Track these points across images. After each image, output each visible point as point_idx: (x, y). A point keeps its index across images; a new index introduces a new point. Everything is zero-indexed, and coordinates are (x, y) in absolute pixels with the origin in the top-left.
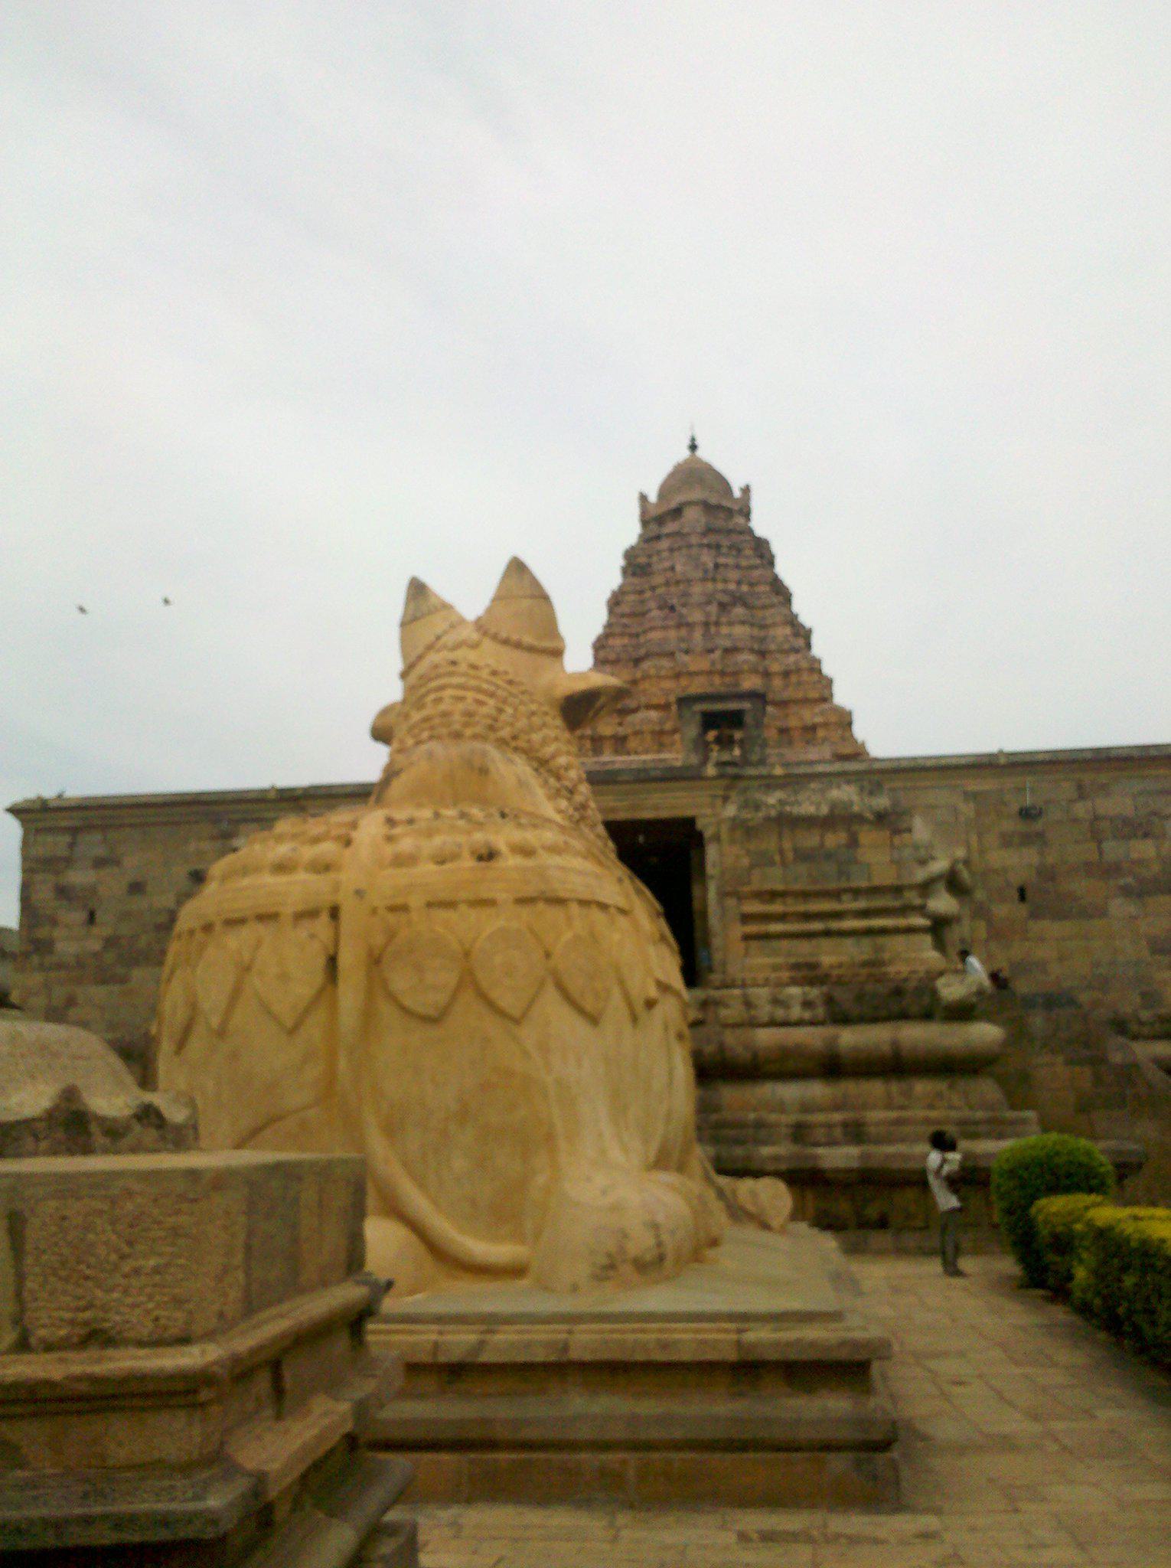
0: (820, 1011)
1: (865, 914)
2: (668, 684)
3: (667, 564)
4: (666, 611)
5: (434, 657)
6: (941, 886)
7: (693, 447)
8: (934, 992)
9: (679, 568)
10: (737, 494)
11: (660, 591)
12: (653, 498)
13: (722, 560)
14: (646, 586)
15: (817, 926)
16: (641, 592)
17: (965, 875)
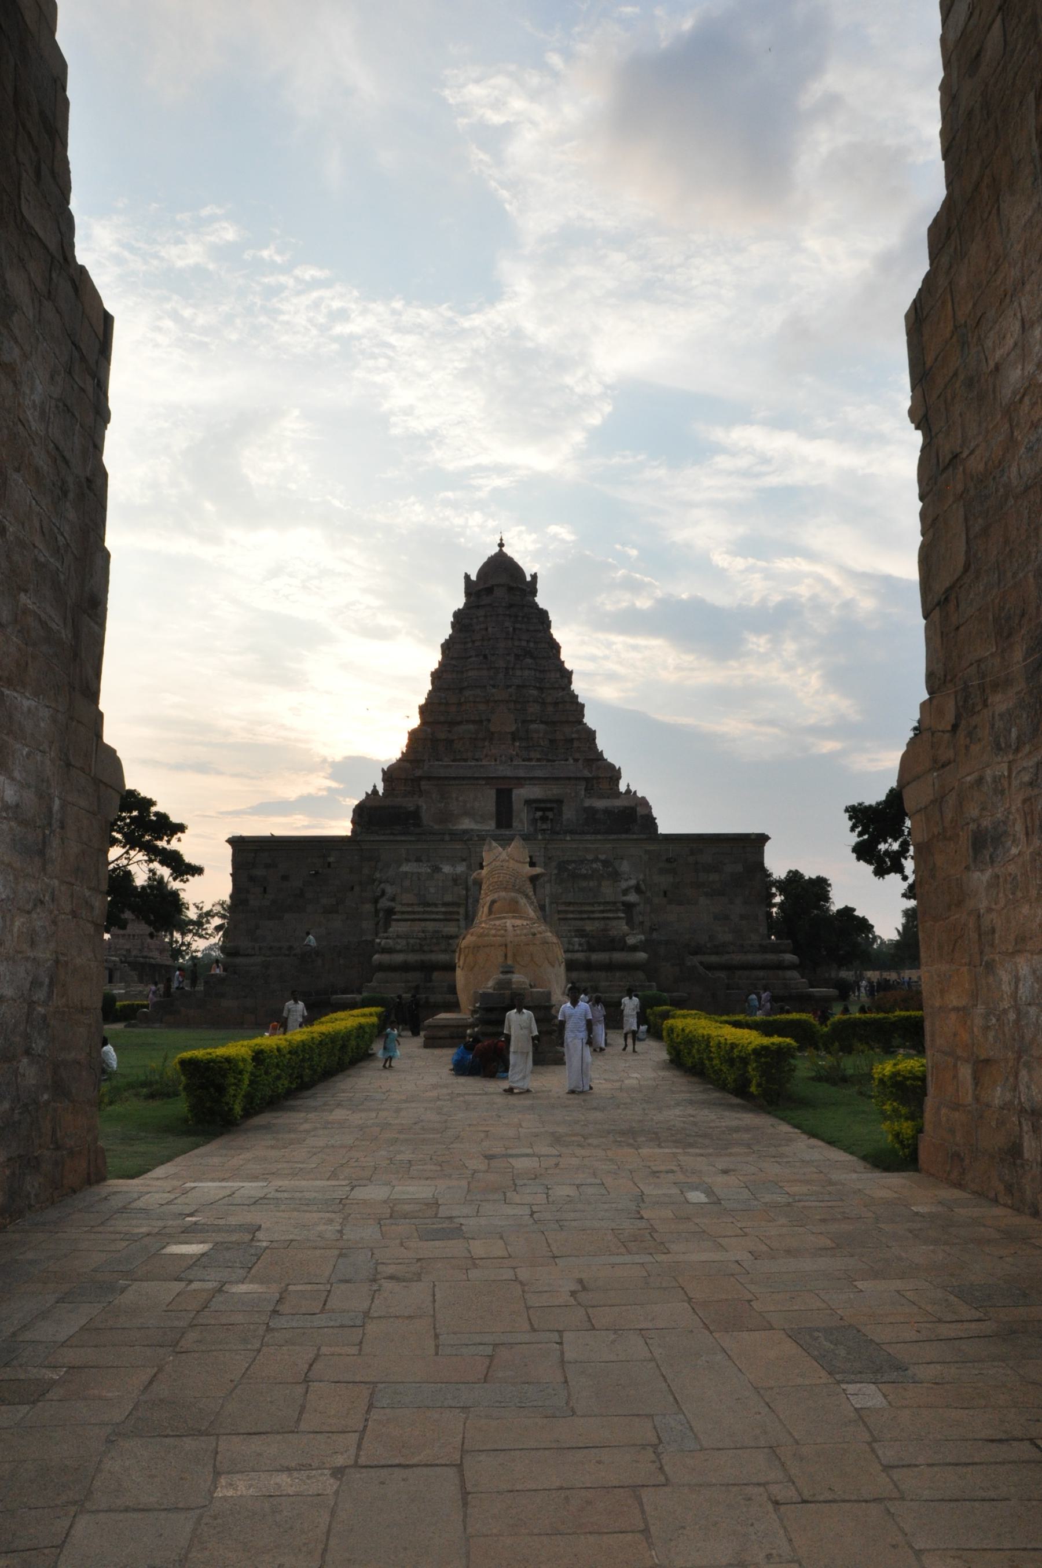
0: (585, 948)
1: (603, 912)
2: (482, 707)
3: (483, 626)
4: (481, 658)
5: (498, 863)
6: (633, 890)
7: (501, 545)
8: (625, 942)
9: (490, 629)
10: (529, 579)
11: (477, 644)
12: (474, 577)
13: (518, 626)
14: (469, 640)
15: (585, 916)
16: (465, 643)
17: (643, 887)
